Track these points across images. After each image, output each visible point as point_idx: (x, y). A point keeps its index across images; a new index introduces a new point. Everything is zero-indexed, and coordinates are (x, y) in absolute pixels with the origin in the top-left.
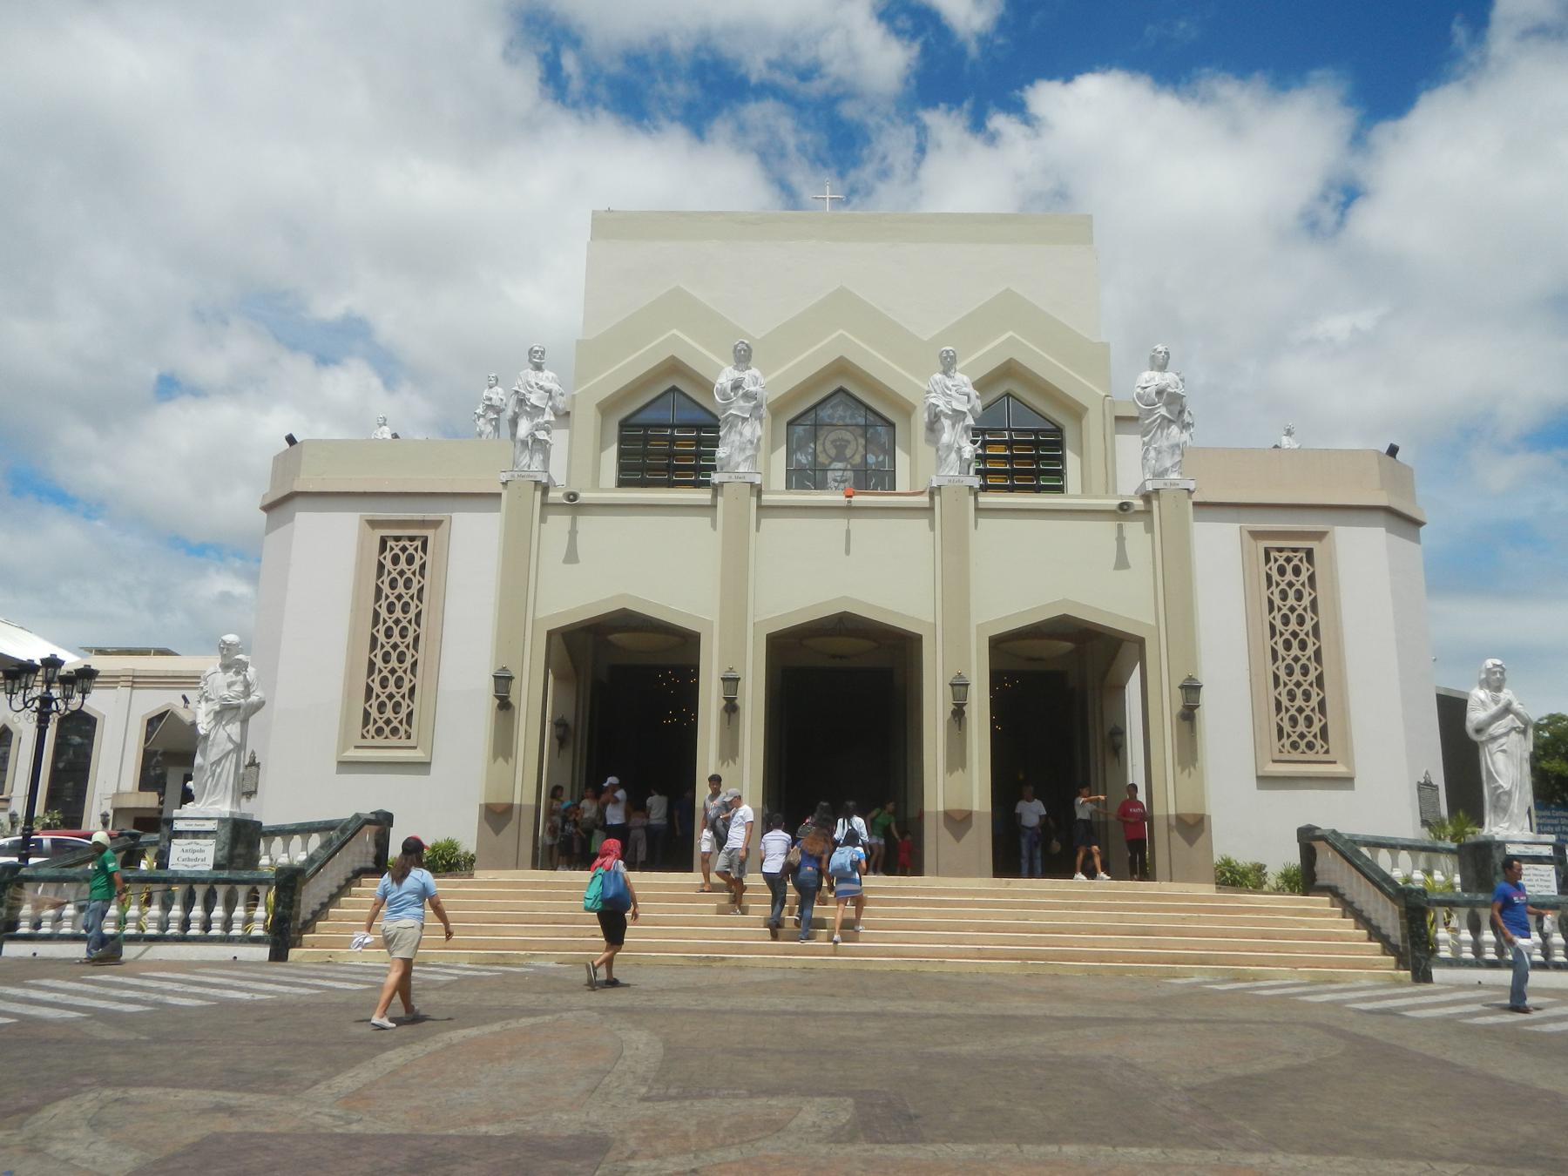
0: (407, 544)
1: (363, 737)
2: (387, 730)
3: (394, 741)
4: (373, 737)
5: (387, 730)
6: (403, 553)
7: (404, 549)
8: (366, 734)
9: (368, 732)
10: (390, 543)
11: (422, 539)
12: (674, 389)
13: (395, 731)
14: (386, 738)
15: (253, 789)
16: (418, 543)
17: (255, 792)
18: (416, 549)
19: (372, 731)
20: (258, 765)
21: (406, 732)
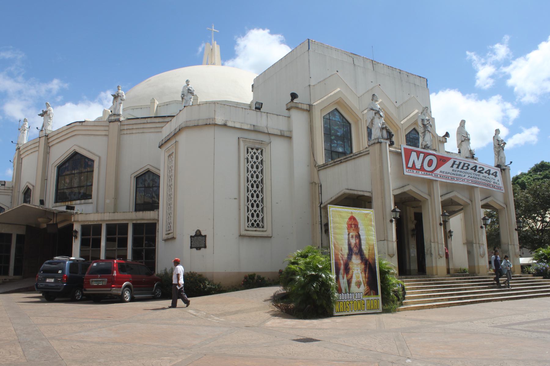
0: (255, 150)
1: (248, 227)
2: (255, 225)
3: (258, 229)
4: (251, 227)
5: (255, 225)
6: (255, 154)
7: (255, 153)
8: (248, 226)
9: (249, 224)
10: (250, 150)
11: (260, 150)
12: (336, 109)
13: (258, 225)
14: (255, 227)
15: (203, 246)
16: (259, 151)
17: (205, 247)
18: (259, 154)
19: (250, 225)
20: (205, 236)
21: (262, 225)
